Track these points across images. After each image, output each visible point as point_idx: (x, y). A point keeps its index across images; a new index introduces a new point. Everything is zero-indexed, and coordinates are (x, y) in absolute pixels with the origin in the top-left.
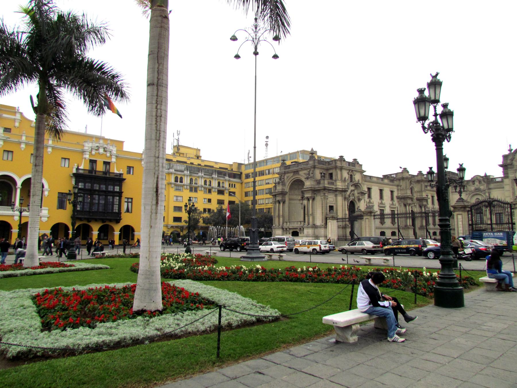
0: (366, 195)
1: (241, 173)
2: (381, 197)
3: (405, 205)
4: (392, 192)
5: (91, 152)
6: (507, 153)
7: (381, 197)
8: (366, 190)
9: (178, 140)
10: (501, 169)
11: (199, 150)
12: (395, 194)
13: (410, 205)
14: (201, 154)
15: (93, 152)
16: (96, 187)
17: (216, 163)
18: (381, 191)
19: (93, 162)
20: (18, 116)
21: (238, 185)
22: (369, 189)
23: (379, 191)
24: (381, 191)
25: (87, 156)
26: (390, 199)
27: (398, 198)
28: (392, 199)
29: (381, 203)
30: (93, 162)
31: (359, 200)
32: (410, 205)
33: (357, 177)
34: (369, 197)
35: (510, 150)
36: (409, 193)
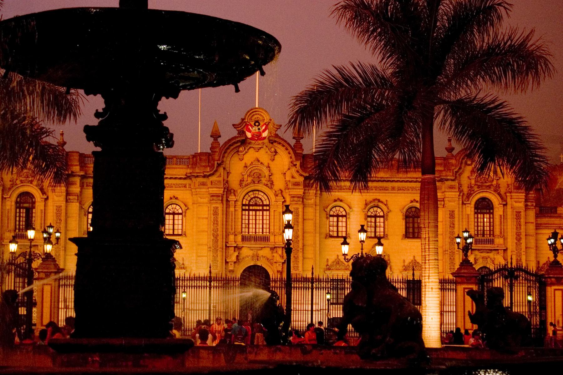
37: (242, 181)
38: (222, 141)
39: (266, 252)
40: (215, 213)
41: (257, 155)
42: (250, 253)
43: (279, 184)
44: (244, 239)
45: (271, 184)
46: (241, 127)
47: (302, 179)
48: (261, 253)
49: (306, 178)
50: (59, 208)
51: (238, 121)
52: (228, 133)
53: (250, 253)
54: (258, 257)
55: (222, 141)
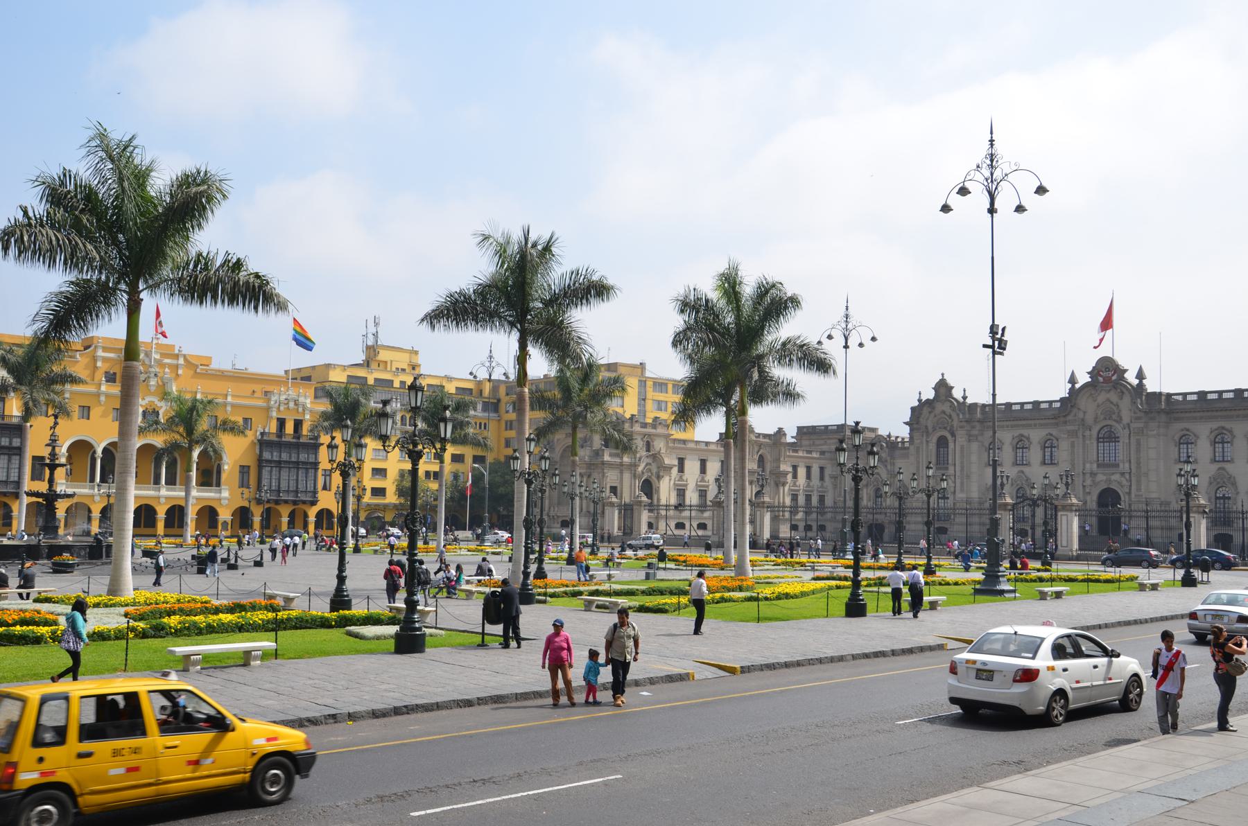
1: (499, 400)
5: (279, 408)
6: (916, 404)
9: (376, 335)
10: (908, 428)
11: (416, 353)
14: (420, 360)
15: (282, 408)
16: (285, 456)
17: (449, 379)
19: (282, 423)
20: (181, 361)
21: (492, 426)
25: (274, 414)
30: (282, 423)
35: (920, 400)
37: (1096, 418)
38: (1077, 386)
39: (1116, 477)
40: (1073, 445)
41: (1108, 396)
42: (1104, 478)
43: (1126, 420)
44: (1099, 466)
45: (1119, 420)
46: (1094, 373)
48: (1113, 477)
50: (962, 447)
51: (1090, 369)
52: (1083, 379)
53: (1104, 478)
54: (1109, 481)
55: (1077, 386)
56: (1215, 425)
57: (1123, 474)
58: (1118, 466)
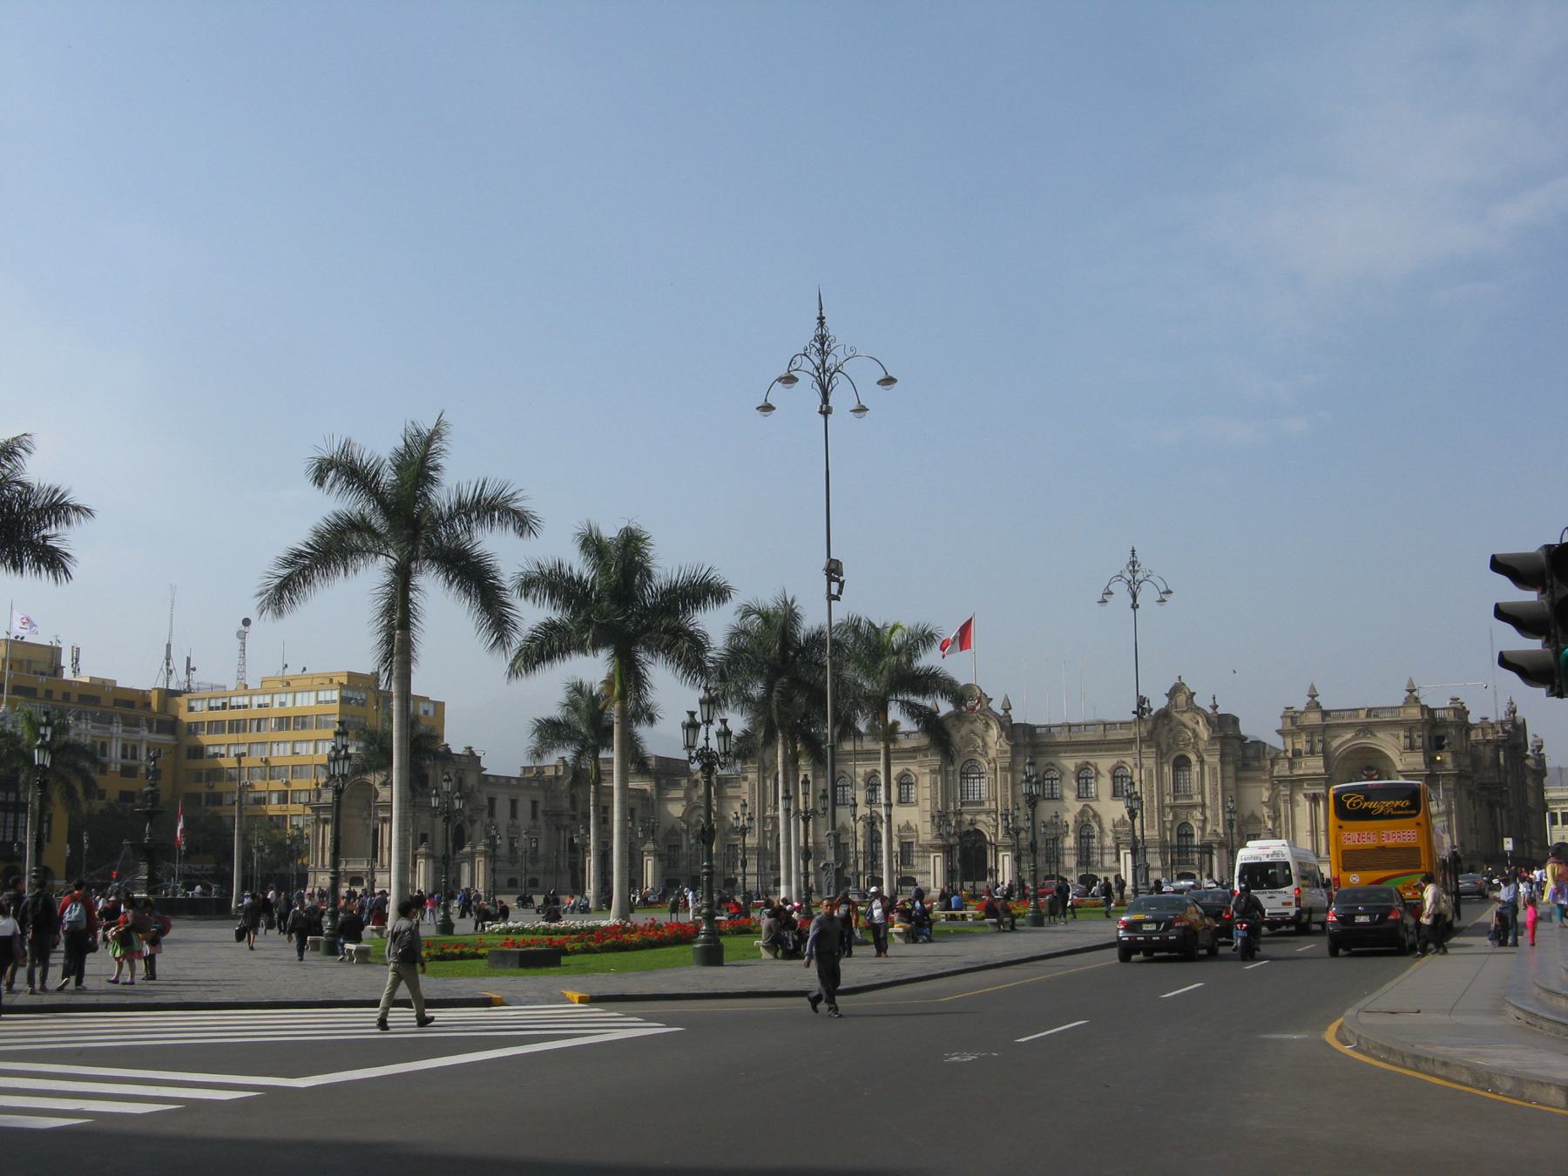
0: (485, 814)
2: (514, 815)
3: (558, 829)
4: (534, 804)
7: (514, 815)
8: (486, 802)
12: (541, 807)
13: (566, 828)
18: (514, 803)
22: (492, 801)
23: (508, 803)
24: (514, 803)
26: (529, 816)
27: (545, 813)
28: (534, 816)
29: (513, 825)
31: (472, 822)
32: (566, 828)
33: (471, 780)
34: (492, 814)
36: (566, 804)
43: (992, 753)
47: (1007, 748)
49: (1013, 747)
56: (1079, 761)
57: (988, 813)
58: (981, 803)
